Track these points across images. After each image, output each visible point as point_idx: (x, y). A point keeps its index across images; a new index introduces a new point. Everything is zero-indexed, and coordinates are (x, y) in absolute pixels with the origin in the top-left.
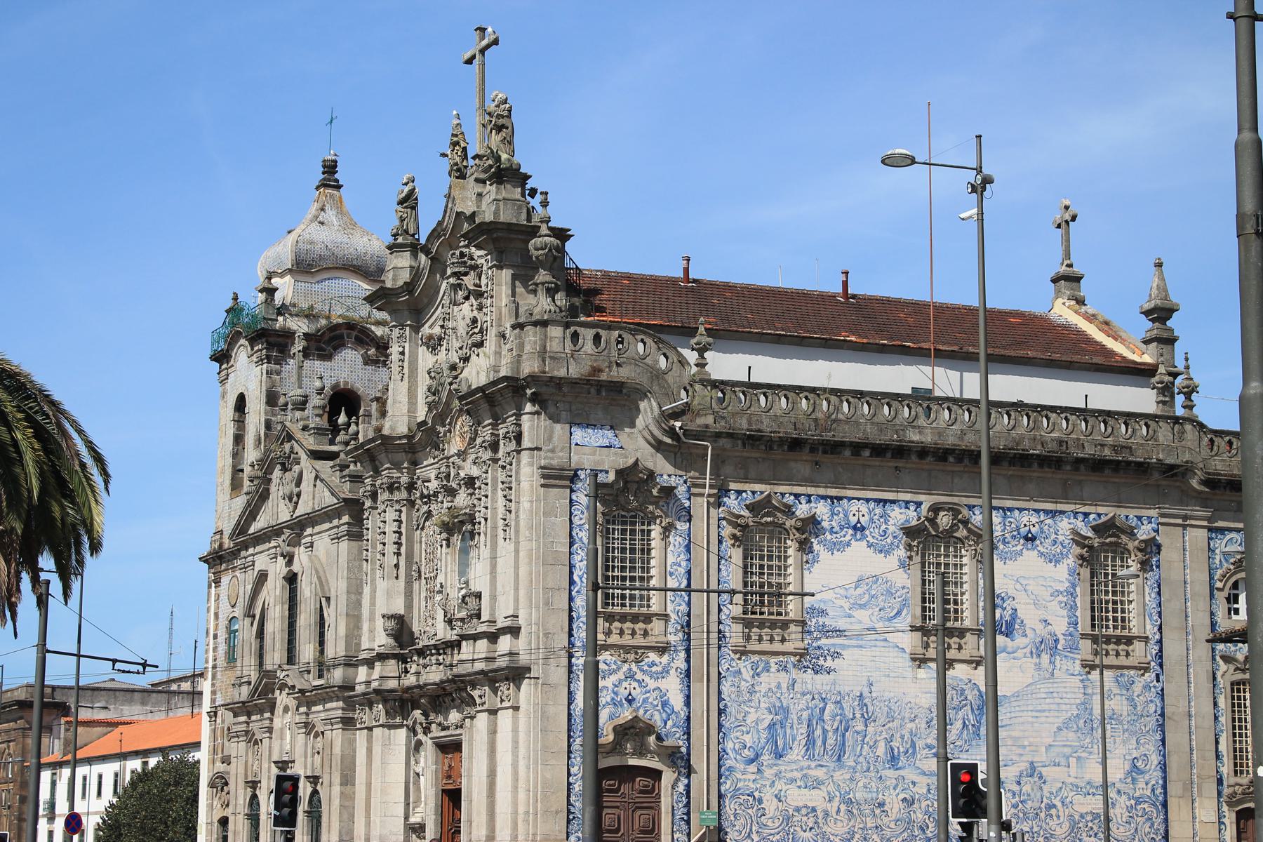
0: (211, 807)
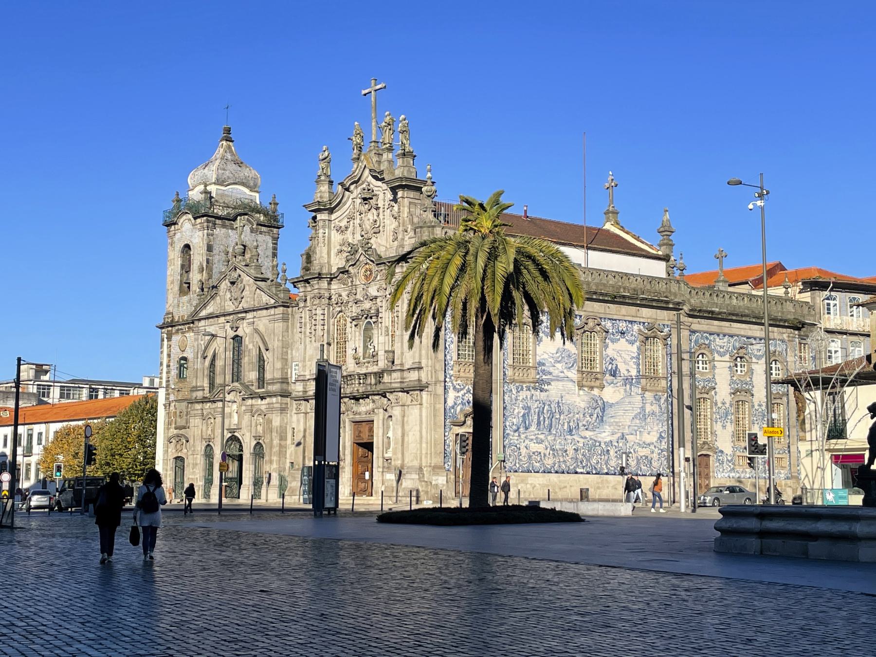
0: (166, 452)
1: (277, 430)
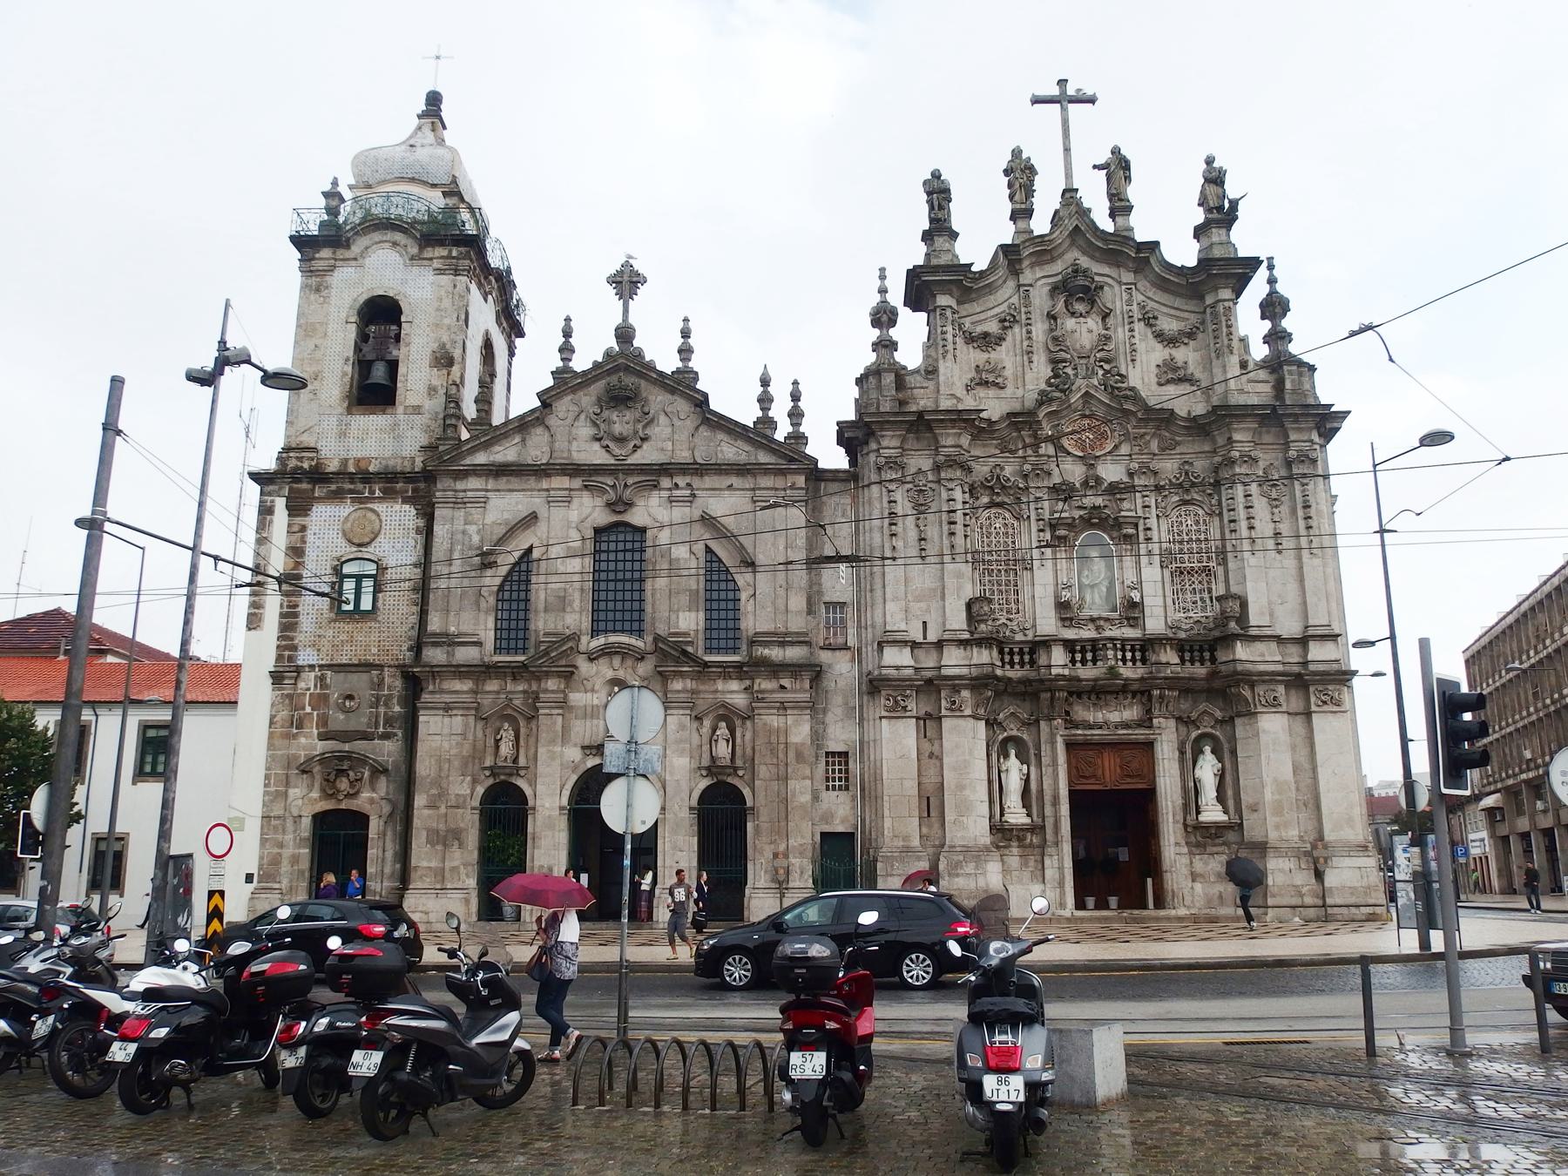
1: (800, 757)
